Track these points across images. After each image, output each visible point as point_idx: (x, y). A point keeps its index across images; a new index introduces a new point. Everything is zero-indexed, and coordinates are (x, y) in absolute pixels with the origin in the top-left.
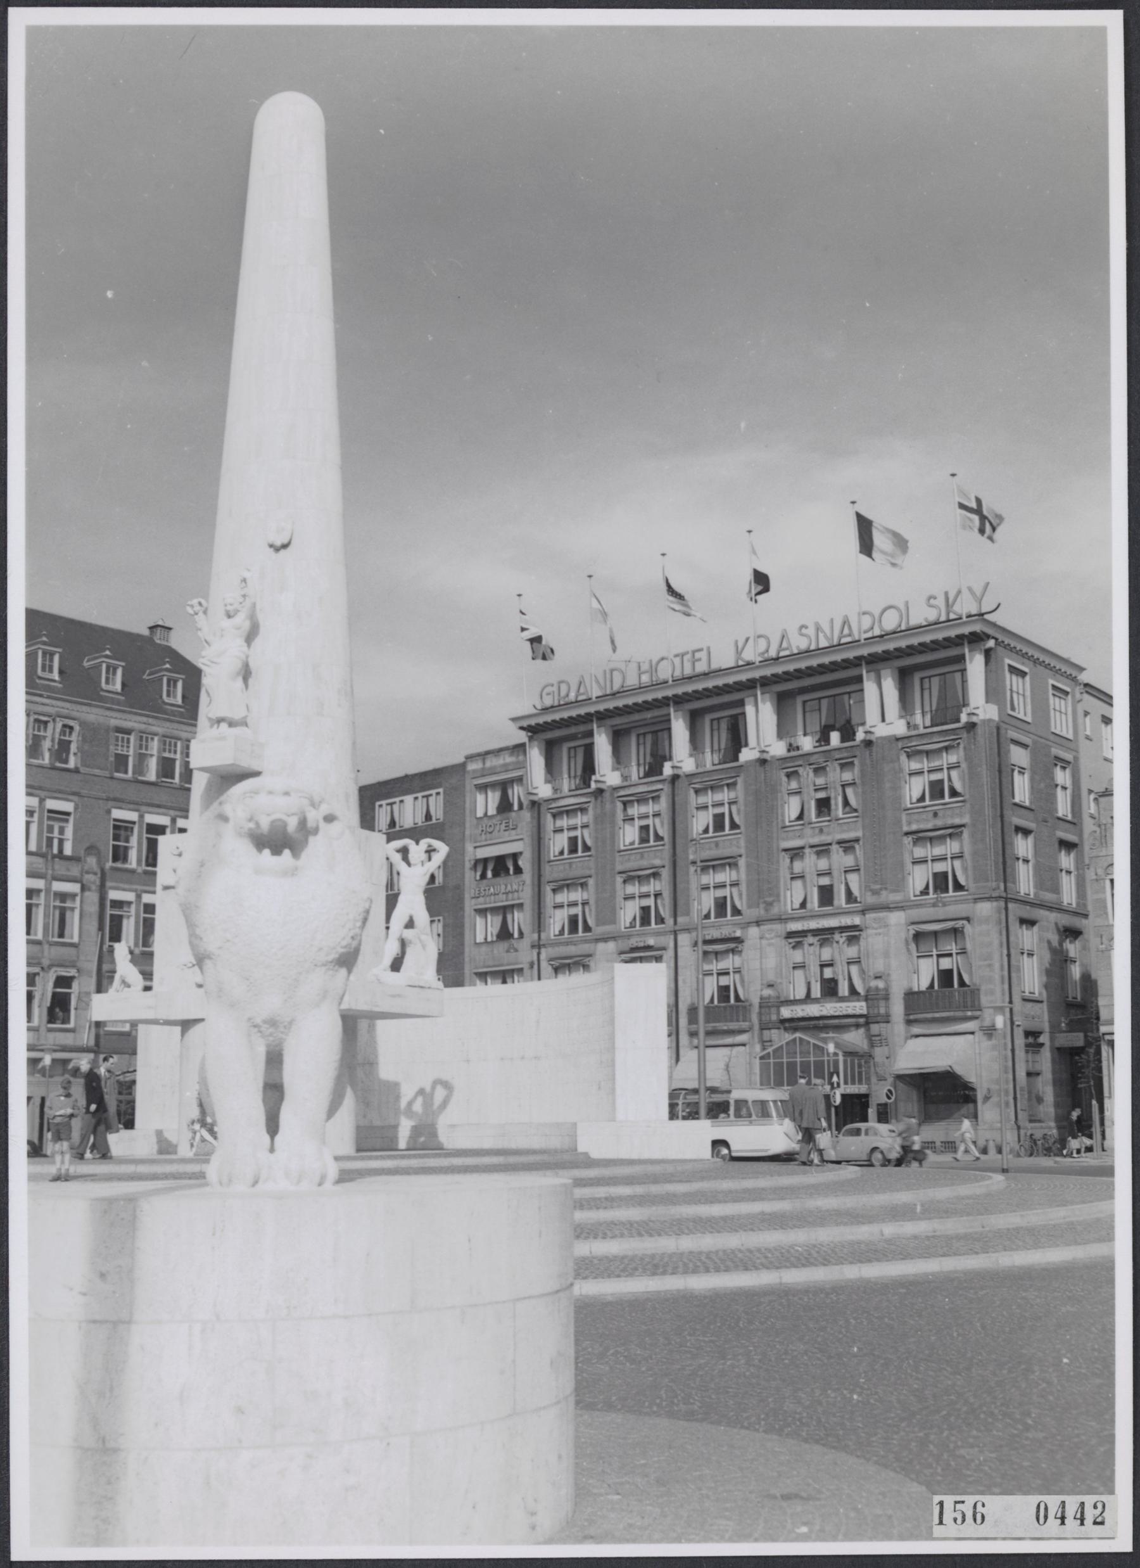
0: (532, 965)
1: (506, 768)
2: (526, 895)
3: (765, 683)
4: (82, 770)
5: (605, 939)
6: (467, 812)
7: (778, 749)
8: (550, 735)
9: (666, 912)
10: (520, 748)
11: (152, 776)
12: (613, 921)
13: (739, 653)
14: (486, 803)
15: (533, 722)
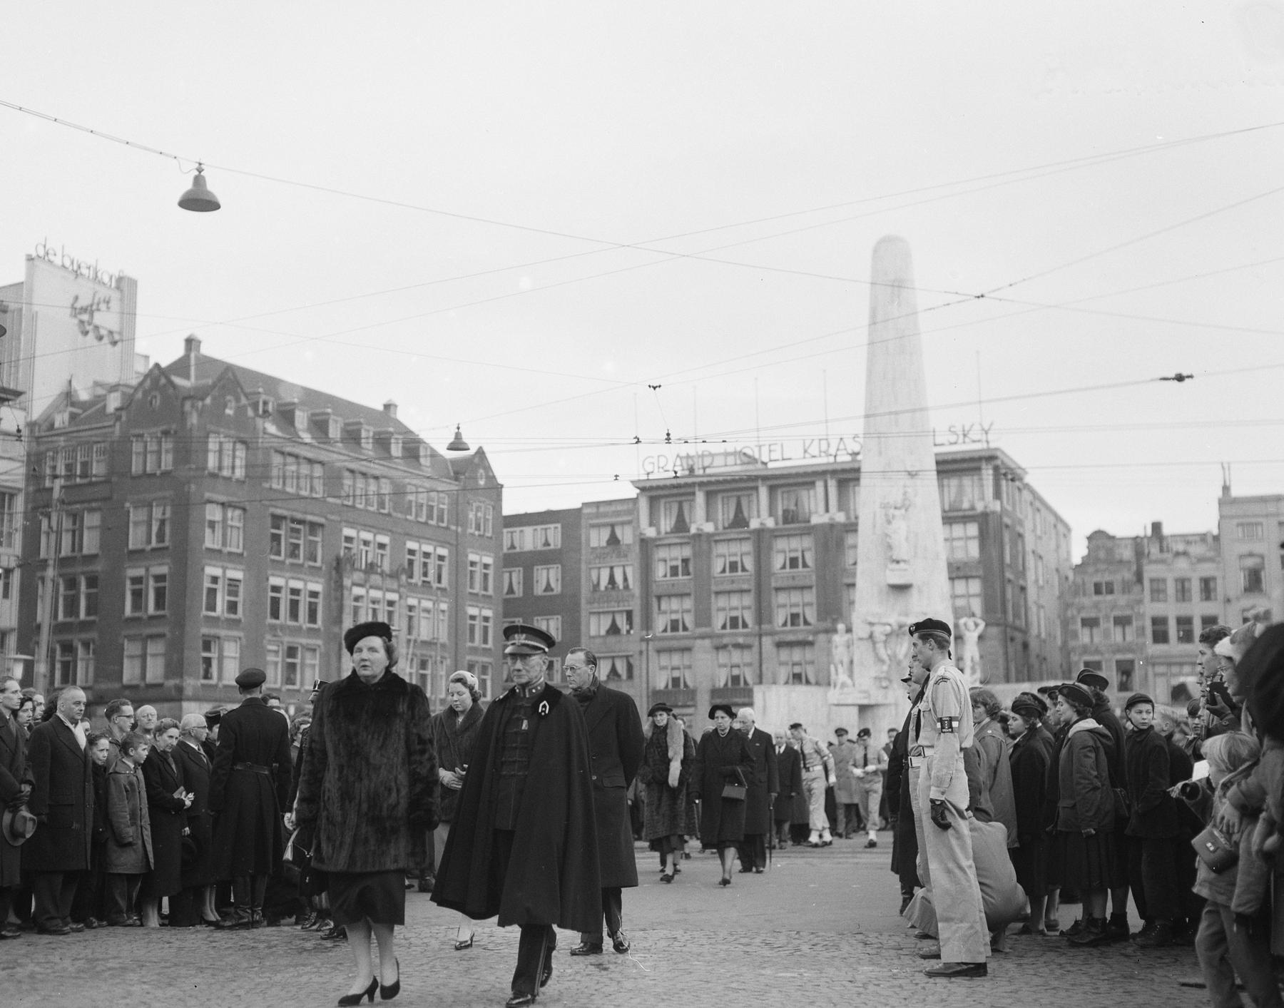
0: (641, 652)
1: (618, 513)
2: (635, 606)
3: (834, 472)
4: (394, 514)
5: (702, 637)
6: (583, 546)
7: (840, 518)
8: (654, 493)
9: (749, 621)
10: (635, 501)
11: (423, 519)
12: (709, 624)
13: (805, 451)
14: (598, 538)
15: (648, 484)
